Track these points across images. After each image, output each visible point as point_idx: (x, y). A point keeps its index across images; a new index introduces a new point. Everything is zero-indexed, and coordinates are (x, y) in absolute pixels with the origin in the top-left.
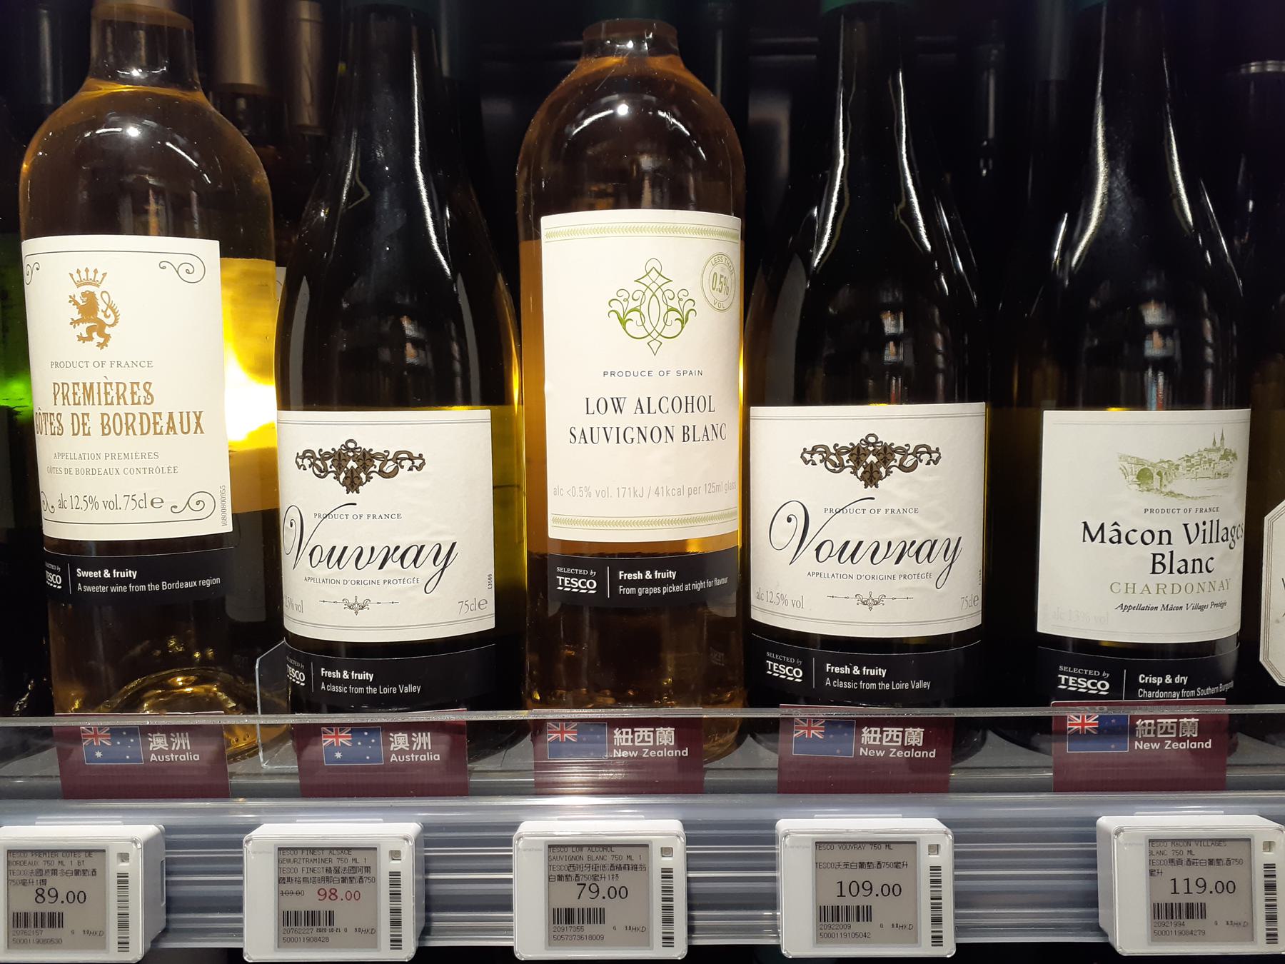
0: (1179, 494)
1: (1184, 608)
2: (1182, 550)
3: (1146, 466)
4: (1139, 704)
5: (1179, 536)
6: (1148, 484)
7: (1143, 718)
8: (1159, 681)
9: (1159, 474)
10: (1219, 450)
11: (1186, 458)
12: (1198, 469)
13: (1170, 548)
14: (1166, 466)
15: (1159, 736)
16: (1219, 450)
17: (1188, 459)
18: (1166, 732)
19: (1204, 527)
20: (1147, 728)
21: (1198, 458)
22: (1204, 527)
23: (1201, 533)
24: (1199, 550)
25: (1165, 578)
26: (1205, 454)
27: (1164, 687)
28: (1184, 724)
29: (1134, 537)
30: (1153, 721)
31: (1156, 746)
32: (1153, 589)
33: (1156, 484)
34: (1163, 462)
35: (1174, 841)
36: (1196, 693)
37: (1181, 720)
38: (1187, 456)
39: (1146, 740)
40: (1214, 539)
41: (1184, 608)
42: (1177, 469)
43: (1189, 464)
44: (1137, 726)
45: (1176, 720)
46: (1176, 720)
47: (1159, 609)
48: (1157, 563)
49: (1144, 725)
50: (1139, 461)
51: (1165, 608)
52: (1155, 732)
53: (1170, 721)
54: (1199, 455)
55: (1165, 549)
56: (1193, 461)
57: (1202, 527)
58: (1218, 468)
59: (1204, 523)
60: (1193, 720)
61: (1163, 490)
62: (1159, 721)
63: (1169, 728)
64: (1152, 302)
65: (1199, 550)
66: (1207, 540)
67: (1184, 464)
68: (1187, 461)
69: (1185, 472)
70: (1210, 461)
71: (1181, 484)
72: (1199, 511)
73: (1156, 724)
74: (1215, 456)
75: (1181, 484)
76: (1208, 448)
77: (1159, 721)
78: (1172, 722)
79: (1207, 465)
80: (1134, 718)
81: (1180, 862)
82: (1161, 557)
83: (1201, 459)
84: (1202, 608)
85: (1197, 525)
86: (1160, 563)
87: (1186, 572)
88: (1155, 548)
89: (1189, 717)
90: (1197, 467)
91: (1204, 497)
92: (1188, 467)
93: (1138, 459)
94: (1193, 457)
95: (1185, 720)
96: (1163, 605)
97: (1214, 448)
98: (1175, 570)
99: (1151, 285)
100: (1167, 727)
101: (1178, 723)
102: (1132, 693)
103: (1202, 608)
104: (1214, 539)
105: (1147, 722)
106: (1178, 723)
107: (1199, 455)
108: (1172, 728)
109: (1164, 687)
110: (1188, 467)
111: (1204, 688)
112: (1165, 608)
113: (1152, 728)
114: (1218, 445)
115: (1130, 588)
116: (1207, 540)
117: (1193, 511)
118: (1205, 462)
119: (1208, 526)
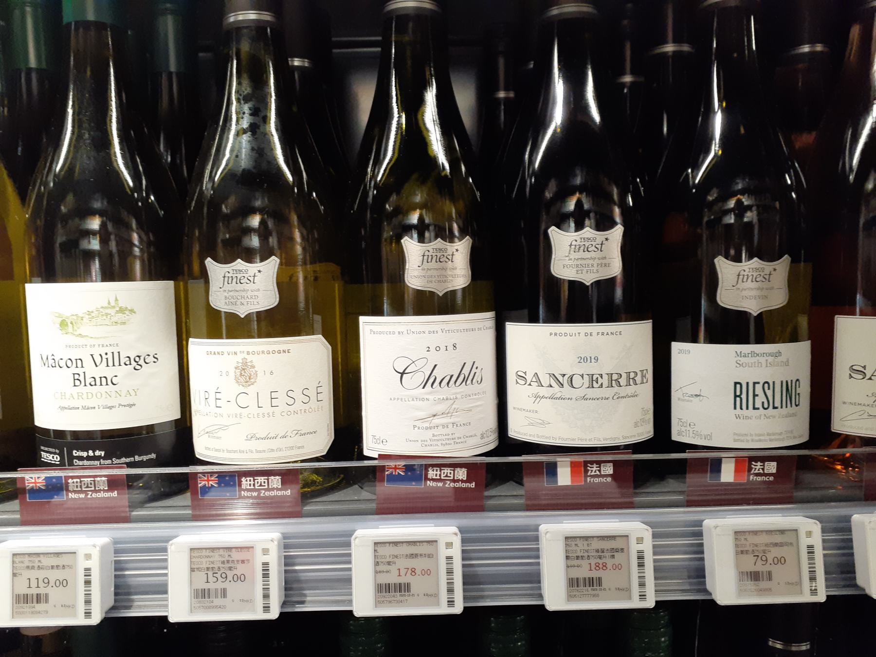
0: (85, 336)
1: (97, 407)
2: (91, 371)
3: (63, 319)
4: (73, 469)
5: (88, 362)
6: (65, 329)
7: (72, 477)
8: (85, 454)
9: (72, 323)
10: (114, 307)
11: (88, 313)
12: (97, 319)
13: (82, 370)
14: (75, 317)
15: (84, 489)
16: (114, 307)
17: (89, 313)
18: (87, 487)
19: (107, 356)
20: (75, 484)
21: (97, 312)
22: (107, 356)
23: (104, 360)
24: (102, 370)
25: (81, 388)
26: (101, 310)
27: (89, 458)
28: (98, 481)
29: (62, 363)
30: (78, 480)
31: (82, 496)
32: (76, 396)
33: (70, 329)
34: (73, 315)
35: (30, 555)
36: (112, 461)
37: (96, 479)
38: (88, 311)
39: (75, 492)
40: (117, 363)
41: (97, 407)
42: (82, 320)
43: (90, 316)
44: (69, 483)
45: (93, 479)
46: (93, 479)
47: (80, 408)
48: (76, 380)
49: (73, 482)
50: (60, 316)
51: (84, 408)
52: (81, 487)
53: (89, 479)
54: (97, 311)
55: (80, 371)
56: (93, 315)
57: (104, 357)
58: (115, 319)
59: (106, 354)
60: (104, 479)
61: (75, 333)
62: (82, 479)
63: (89, 484)
64: (97, 216)
65: (102, 370)
66: (111, 363)
67: (87, 316)
68: (89, 315)
69: (88, 322)
70: (107, 314)
71: (86, 329)
72: (101, 346)
73: (81, 482)
74: (112, 312)
75: (86, 329)
76: (104, 306)
77: (82, 479)
78: (91, 481)
79: (105, 317)
80: (67, 478)
81: (33, 567)
82: (78, 376)
83: (99, 313)
84: (110, 408)
85: (100, 355)
86: (78, 379)
87: (95, 385)
88: (74, 370)
89: (101, 476)
90: (96, 318)
91: (105, 337)
92: (89, 318)
93: (60, 314)
94: (92, 312)
95: (99, 479)
96: (82, 406)
97: (110, 306)
98: (87, 384)
99: (97, 205)
100: (88, 483)
101: (94, 481)
102: (71, 464)
103: (110, 408)
104: (117, 363)
105: (75, 480)
106: (94, 481)
107: (97, 311)
108: (91, 484)
109: (89, 458)
110: (89, 318)
111: (119, 458)
112: (84, 408)
113: (79, 484)
114: (113, 303)
115: (63, 395)
116: (111, 363)
117: (97, 346)
118: (103, 315)
119: (110, 356)
